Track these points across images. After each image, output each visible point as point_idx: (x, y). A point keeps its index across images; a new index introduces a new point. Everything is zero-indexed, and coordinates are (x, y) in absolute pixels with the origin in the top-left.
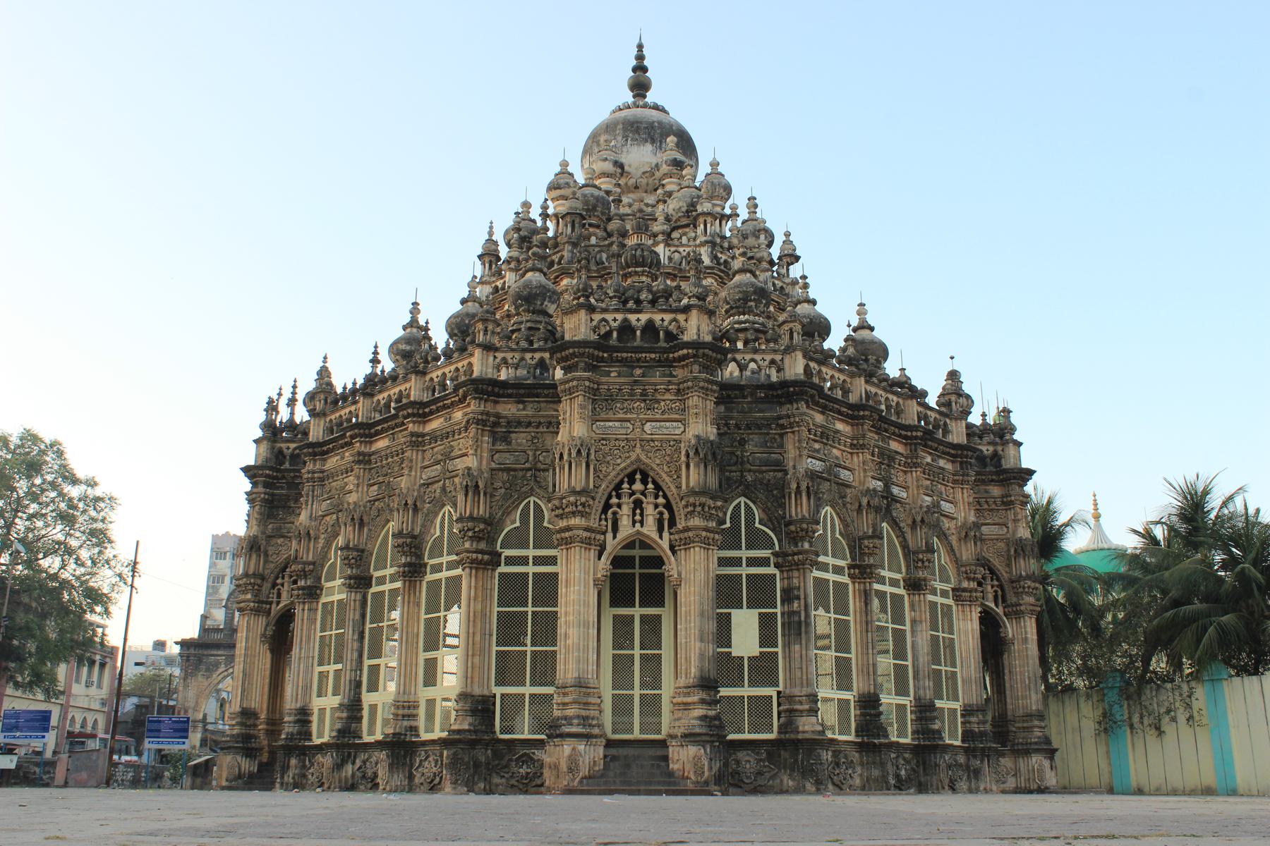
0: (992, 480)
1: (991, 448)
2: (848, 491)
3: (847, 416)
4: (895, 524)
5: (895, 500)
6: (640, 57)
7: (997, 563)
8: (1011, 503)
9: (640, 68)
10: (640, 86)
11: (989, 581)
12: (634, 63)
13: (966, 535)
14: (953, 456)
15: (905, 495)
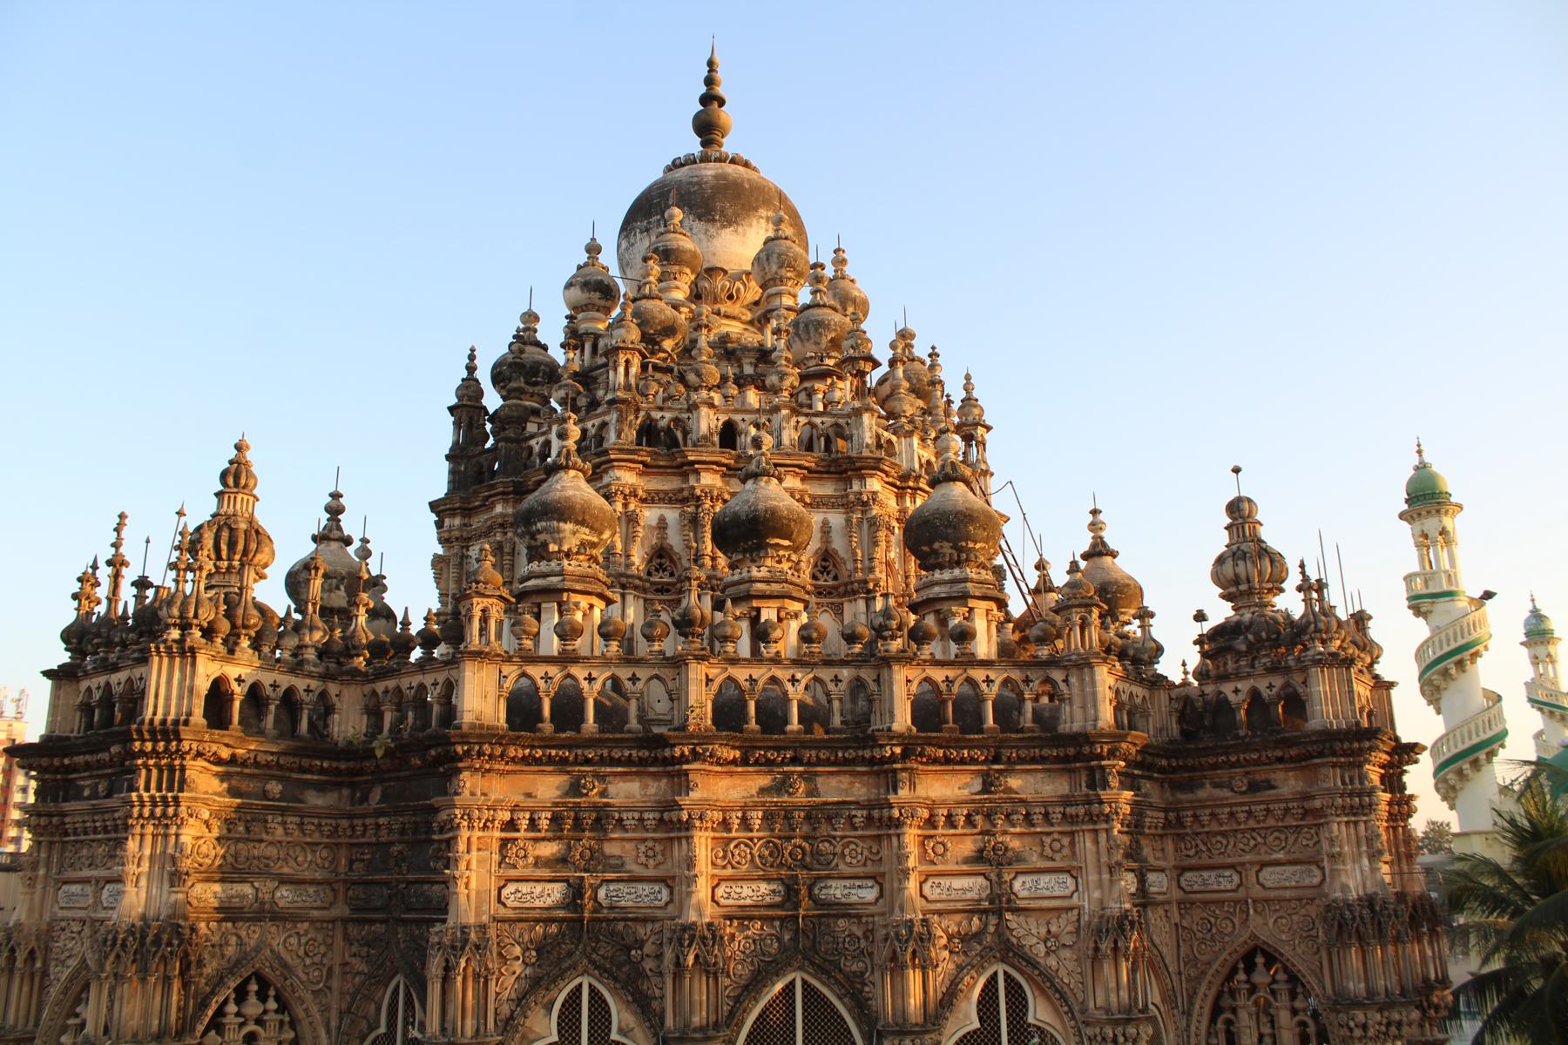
0: (1280, 760)
1: (1278, 681)
2: (642, 931)
3: (642, 762)
4: (825, 970)
5: (843, 910)
6: (710, 82)
7: (1297, 955)
8: (1318, 813)
9: (711, 99)
10: (707, 129)
11: (1284, 999)
12: (703, 89)
13: (1097, 949)
14: (1058, 759)
15: (870, 894)
